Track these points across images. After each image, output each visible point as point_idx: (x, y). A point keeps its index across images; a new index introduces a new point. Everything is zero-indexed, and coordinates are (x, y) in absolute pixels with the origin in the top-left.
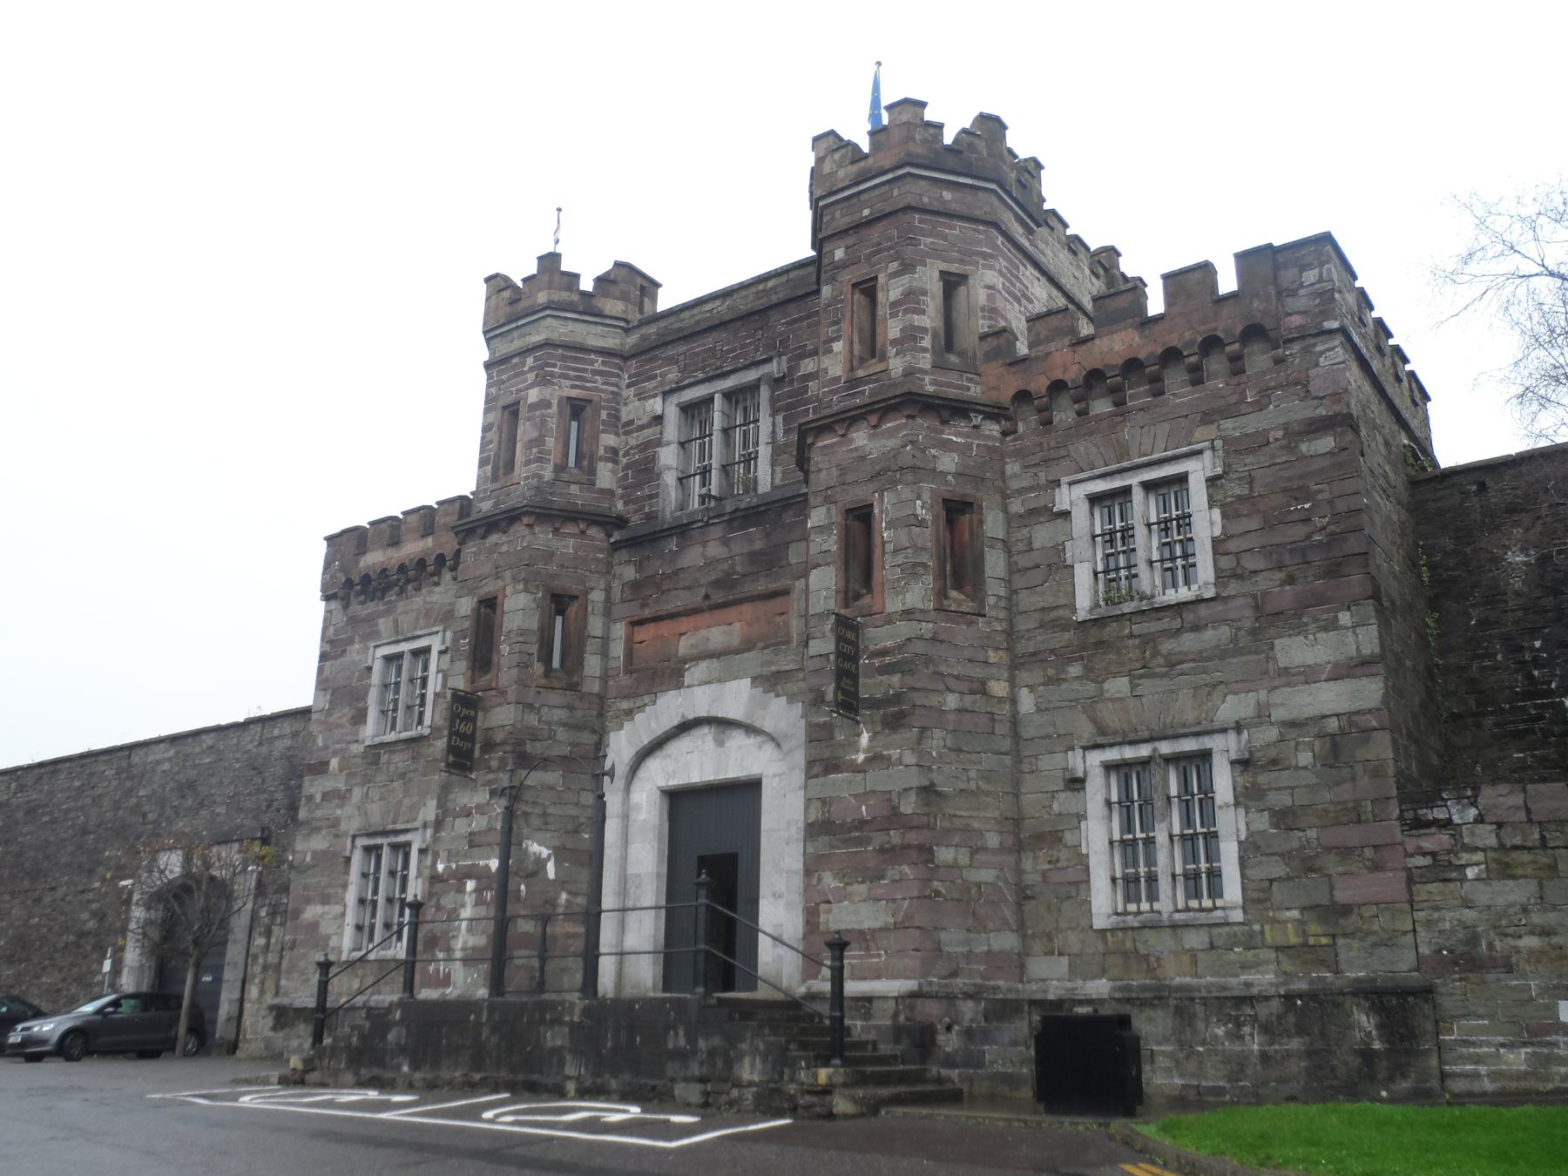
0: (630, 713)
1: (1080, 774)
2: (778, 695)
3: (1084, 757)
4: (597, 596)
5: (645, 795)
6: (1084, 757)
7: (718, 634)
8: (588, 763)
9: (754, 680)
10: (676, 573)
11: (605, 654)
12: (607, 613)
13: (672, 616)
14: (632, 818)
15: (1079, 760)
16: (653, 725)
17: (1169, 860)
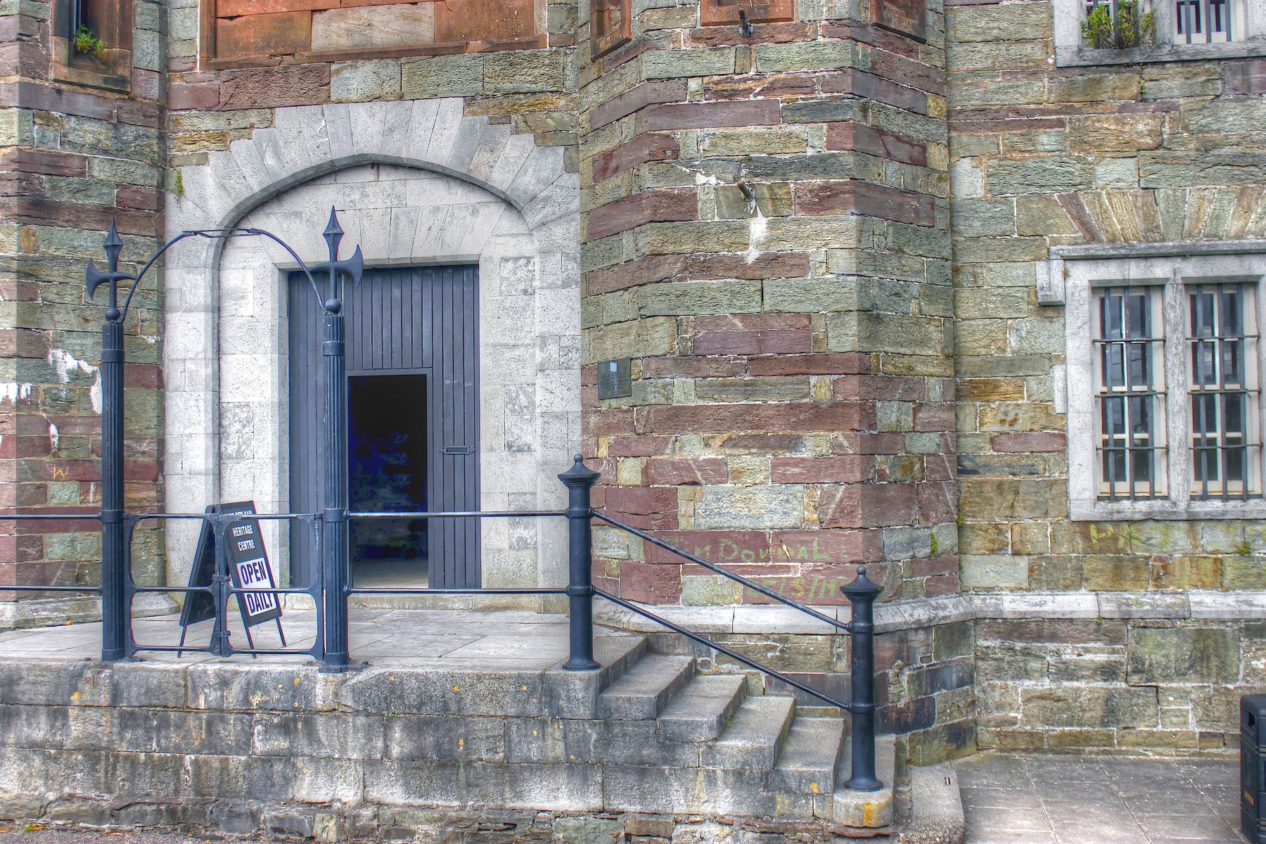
0: (221, 139)
1: (1059, 297)
2: (517, 131)
3: (1066, 275)
5: (250, 275)
6: (1066, 275)
8: (141, 213)
9: (470, 100)
11: (164, 31)
14: (225, 313)
15: (1057, 277)
16: (270, 161)
17: (1173, 427)
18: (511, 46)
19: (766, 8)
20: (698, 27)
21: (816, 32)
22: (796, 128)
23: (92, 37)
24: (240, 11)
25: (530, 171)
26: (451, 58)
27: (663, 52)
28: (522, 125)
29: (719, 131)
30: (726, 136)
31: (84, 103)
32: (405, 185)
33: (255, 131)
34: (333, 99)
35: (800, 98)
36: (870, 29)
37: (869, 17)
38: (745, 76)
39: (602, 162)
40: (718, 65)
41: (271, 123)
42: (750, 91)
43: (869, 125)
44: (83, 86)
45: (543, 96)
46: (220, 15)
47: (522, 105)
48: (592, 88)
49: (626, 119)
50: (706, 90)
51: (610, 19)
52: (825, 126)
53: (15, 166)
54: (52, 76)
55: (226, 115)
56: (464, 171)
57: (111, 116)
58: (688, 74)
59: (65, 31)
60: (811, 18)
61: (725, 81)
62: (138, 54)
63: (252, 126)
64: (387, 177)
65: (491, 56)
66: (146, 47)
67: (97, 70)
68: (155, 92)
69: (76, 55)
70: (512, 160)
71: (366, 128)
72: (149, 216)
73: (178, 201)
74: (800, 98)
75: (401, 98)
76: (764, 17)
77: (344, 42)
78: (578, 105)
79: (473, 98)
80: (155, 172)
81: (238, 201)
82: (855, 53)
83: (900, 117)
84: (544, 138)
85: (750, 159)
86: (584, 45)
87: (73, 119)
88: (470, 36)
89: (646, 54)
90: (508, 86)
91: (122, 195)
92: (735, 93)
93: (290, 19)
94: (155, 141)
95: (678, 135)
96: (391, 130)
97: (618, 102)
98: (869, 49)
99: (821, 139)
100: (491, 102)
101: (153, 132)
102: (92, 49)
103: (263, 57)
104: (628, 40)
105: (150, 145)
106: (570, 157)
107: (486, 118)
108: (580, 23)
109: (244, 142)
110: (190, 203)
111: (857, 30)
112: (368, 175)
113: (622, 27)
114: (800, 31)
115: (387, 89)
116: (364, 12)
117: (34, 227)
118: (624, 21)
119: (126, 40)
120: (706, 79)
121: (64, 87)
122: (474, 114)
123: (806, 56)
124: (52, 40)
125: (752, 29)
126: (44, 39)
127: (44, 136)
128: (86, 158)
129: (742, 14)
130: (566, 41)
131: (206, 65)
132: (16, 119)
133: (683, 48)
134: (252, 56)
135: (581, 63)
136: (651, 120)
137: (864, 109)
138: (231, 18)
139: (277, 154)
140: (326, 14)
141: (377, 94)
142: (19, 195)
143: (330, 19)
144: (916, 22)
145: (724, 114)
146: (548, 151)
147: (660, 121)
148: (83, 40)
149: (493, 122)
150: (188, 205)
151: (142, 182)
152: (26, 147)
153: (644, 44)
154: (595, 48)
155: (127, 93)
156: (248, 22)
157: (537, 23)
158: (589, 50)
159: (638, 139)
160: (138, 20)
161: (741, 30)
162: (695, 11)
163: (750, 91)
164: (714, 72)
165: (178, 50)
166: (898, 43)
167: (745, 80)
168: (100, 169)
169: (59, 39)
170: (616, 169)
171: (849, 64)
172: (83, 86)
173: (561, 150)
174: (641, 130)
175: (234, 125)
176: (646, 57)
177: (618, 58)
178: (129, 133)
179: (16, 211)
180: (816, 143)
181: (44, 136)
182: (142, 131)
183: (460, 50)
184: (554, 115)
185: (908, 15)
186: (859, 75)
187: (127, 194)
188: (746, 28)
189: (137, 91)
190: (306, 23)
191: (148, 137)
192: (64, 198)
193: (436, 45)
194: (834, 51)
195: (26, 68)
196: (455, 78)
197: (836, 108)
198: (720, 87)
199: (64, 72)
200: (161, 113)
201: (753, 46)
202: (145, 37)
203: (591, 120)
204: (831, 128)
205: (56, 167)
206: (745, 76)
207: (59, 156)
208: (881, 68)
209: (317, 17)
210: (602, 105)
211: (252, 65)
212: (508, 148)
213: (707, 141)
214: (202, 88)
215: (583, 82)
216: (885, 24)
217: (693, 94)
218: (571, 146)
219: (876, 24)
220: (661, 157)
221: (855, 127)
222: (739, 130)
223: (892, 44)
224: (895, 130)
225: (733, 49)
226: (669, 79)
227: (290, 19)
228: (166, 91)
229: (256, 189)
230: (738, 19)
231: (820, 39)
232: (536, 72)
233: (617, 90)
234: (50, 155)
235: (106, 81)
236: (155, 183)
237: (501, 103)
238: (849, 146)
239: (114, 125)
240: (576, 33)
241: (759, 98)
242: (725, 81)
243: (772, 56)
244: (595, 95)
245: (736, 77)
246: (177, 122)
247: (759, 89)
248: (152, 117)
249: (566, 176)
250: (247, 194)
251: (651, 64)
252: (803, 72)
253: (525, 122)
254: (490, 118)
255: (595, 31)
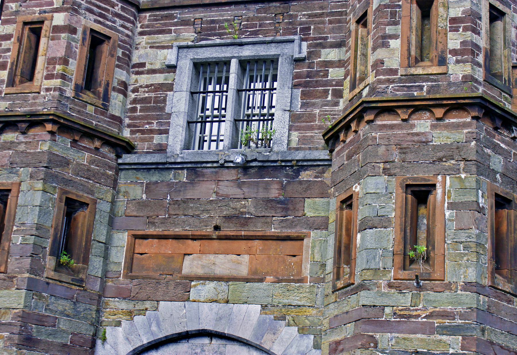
0: (130, 314)
2: (289, 325)
4: (104, 207)
7: (223, 263)
9: (264, 307)
10: (185, 201)
11: (106, 257)
12: (111, 224)
13: (177, 237)
16: (154, 328)
18: (289, 281)
19: (429, 274)
20: (392, 281)
21: (457, 288)
22: (444, 338)
23: (69, 257)
24: (146, 251)
25: (294, 346)
26: (256, 284)
27: (371, 292)
28: (292, 322)
29: (401, 335)
30: (404, 339)
31: (60, 290)
32: (225, 347)
33: (147, 312)
34: (191, 299)
35: (447, 322)
36: (487, 288)
37: (486, 282)
38: (416, 308)
39: (334, 345)
40: (402, 301)
41: (157, 309)
42: (418, 316)
43: (485, 339)
44: (60, 281)
45: (304, 308)
46: (136, 251)
47: (292, 312)
48: (332, 306)
49: (349, 325)
50: (395, 314)
51: (344, 272)
52: (460, 338)
53: (20, 319)
54: (45, 275)
55: (133, 303)
56: (258, 343)
57: (73, 298)
58: (385, 304)
59: (55, 253)
60: (455, 281)
61: (405, 310)
62: (91, 268)
63: (146, 309)
64: (215, 342)
65: (278, 285)
66: (96, 265)
67: (69, 274)
68: (97, 287)
69: (59, 266)
70: (285, 340)
71: (207, 317)
72: (86, 350)
73: (103, 344)
74: (447, 322)
75: (227, 302)
76: (428, 278)
77: (200, 272)
78: (323, 314)
79: (266, 306)
80: (92, 328)
81: (134, 347)
82: (478, 301)
83: (503, 336)
84: (303, 331)
85: (418, 352)
86: (328, 284)
87: (53, 298)
88: (267, 274)
89: (362, 292)
90: (286, 301)
91: (73, 338)
92: (410, 316)
93: (173, 257)
94: (94, 312)
95: (378, 336)
96: (220, 319)
97: (345, 315)
98: (486, 299)
99: (458, 344)
100: (275, 309)
101: (94, 307)
102: (68, 264)
103: (157, 275)
104: (353, 284)
105: (91, 314)
106: (317, 341)
107: (272, 317)
108: (327, 272)
109: (141, 317)
110: (109, 346)
111: (480, 288)
112: (206, 341)
113: (350, 277)
114: (448, 287)
115: (220, 297)
116: (212, 257)
117: (25, 351)
118: (352, 274)
119: (86, 260)
120: (395, 308)
121: (51, 281)
122: (266, 314)
123: (451, 300)
124: (48, 258)
125: (421, 284)
126: (44, 258)
127: (37, 305)
128: (57, 318)
129: (417, 276)
130: (319, 280)
131: (126, 276)
132: (23, 295)
133: (383, 291)
134: (151, 274)
135: (326, 293)
136: (363, 326)
137: (483, 331)
138: (141, 254)
139: (158, 325)
140: (191, 256)
141: (215, 298)
142: (19, 334)
143: (193, 259)
144: (513, 286)
145: (404, 327)
146: (305, 337)
147: (368, 327)
148: (64, 259)
149: (277, 319)
150: (107, 346)
151: (84, 333)
152: (27, 310)
153: (362, 287)
154: (334, 286)
155: (83, 287)
156: (150, 257)
157: (303, 270)
158: (331, 286)
159: (355, 336)
160: (93, 251)
161: (415, 284)
162: (390, 272)
163: (418, 316)
164: (399, 304)
165: (112, 268)
166: (503, 297)
167: (416, 310)
168: (63, 324)
169: (51, 257)
170: (342, 351)
171: (475, 306)
172: (60, 281)
173: (312, 337)
174: (357, 331)
175: (137, 308)
176: (362, 293)
177: (346, 293)
178: (81, 307)
179: (16, 342)
180: (455, 347)
181: (37, 305)
182: (88, 306)
183: (261, 280)
184: (310, 318)
185: (509, 282)
186: (480, 312)
187: (76, 338)
188: (418, 283)
189: (88, 286)
190: (180, 260)
191: (91, 310)
192: (43, 338)
193: (250, 277)
194: (469, 299)
195: (32, 271)
196: (257, 295)
197: (467, 328)
198: (402, 313)
199: (52, 274)
200: (99, 299)
201: (422, 293)
202: (96, 260)
203: (330, 323)
204: (463, 339)
205: (41, 321)
206: (416, 308)
207: (43, 316)
208: (493, 309)
209: (187, 257)
210: (337, 316)
211: (150, 278)
212: (283, 333)
213: (394, 340)
214: (122, 288)
215: (326, 303)
216: (496, 286)
217: (387, 315)
218: (318, 335)
219: (490, 286)
220: (368, 346)
221: (477, 339)
222: (412, 336)
223: (499, 297)
224: (500, 342)
225: (411, 293)
226: (374, 306)
227: (173, 257)
228: (103, 288)
229: (145, 342)
230: (414, 278)
231: (459, 292)
232: (301, 295)
233: (345, 309)
234: (39, 315)
235: (72, 280)
236: (92, 334)
237: (281, 310)
238: (474, 350)
239: (74, 302)
240: (324, 277)
241: (424, 320)
242: (405, 310)
243: (432, 299)
244: (333, 310)
245: (412, 308)
246: (107, 304)
247: (424, 315)
248: (94, 300)
249: (314, 351)
250: (140, 344)
251: (365, 298)
252: (449, 308)
253: (294, 320)
254: (275, 317)
255: (335, 277)
